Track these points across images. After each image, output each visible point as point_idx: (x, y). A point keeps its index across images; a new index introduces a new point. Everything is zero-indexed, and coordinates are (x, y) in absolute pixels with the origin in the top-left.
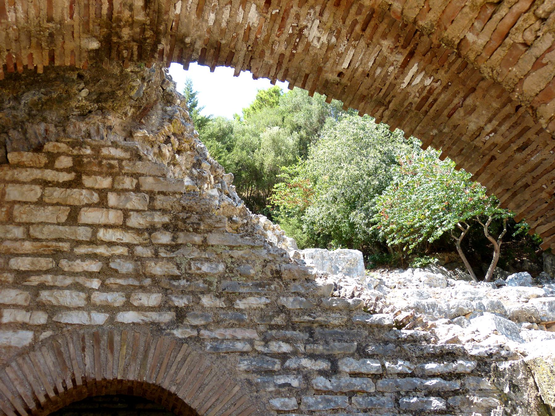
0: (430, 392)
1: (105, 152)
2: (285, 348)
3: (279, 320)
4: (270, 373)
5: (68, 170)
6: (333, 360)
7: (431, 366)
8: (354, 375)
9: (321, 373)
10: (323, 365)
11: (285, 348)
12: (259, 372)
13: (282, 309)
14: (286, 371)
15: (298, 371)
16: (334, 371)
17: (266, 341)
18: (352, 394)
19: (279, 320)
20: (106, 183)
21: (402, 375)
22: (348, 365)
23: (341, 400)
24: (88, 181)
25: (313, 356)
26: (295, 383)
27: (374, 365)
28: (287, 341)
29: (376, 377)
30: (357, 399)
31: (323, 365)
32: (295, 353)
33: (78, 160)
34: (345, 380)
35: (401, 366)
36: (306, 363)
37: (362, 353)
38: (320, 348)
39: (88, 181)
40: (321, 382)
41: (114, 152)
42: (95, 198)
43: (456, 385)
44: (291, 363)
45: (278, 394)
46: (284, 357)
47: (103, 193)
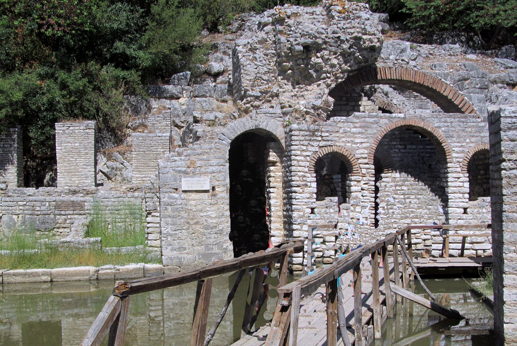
0: (427, 153)
1: (353, 95)
2: (395, 143)
3: (394, 137)
4: (392, 149)
5: (345, 101)
6: (405, 145)
7: (427, 147)
8: (410, 149)
9: (403, 148)
10: (403, 147)
11: (395, 143)
12: (389, 148)
13: (394, 134)
14: (395, 148)
15: (398, 148)
16: (405, 148)
17: (391, 141)
18: (409, 153)
19: (394, 137)
20: (354, 104)
21: (420, 149)
22: (409, 147)
23: (407, 154)
24: (350, 104)
25: (400, 145)
26: (397, 151)
27: (414, 147)
28: (396, 141)
29: (414, 149)
30: (410, 154)
31: (403, 147)
32: (397, 144)
33: (347, 98)
34: (408, 150)
35: (421, 147)
36: (399, 146)
37: (412, 144)
38: (402, 143)
39: (350, 104)
40: (403, 151)
41: (355, 95)
42: (352, 108)
43: (433, 151)
44: (396, 147)
45: (393, 153)
46: (395, 145)
47: (354, 106)
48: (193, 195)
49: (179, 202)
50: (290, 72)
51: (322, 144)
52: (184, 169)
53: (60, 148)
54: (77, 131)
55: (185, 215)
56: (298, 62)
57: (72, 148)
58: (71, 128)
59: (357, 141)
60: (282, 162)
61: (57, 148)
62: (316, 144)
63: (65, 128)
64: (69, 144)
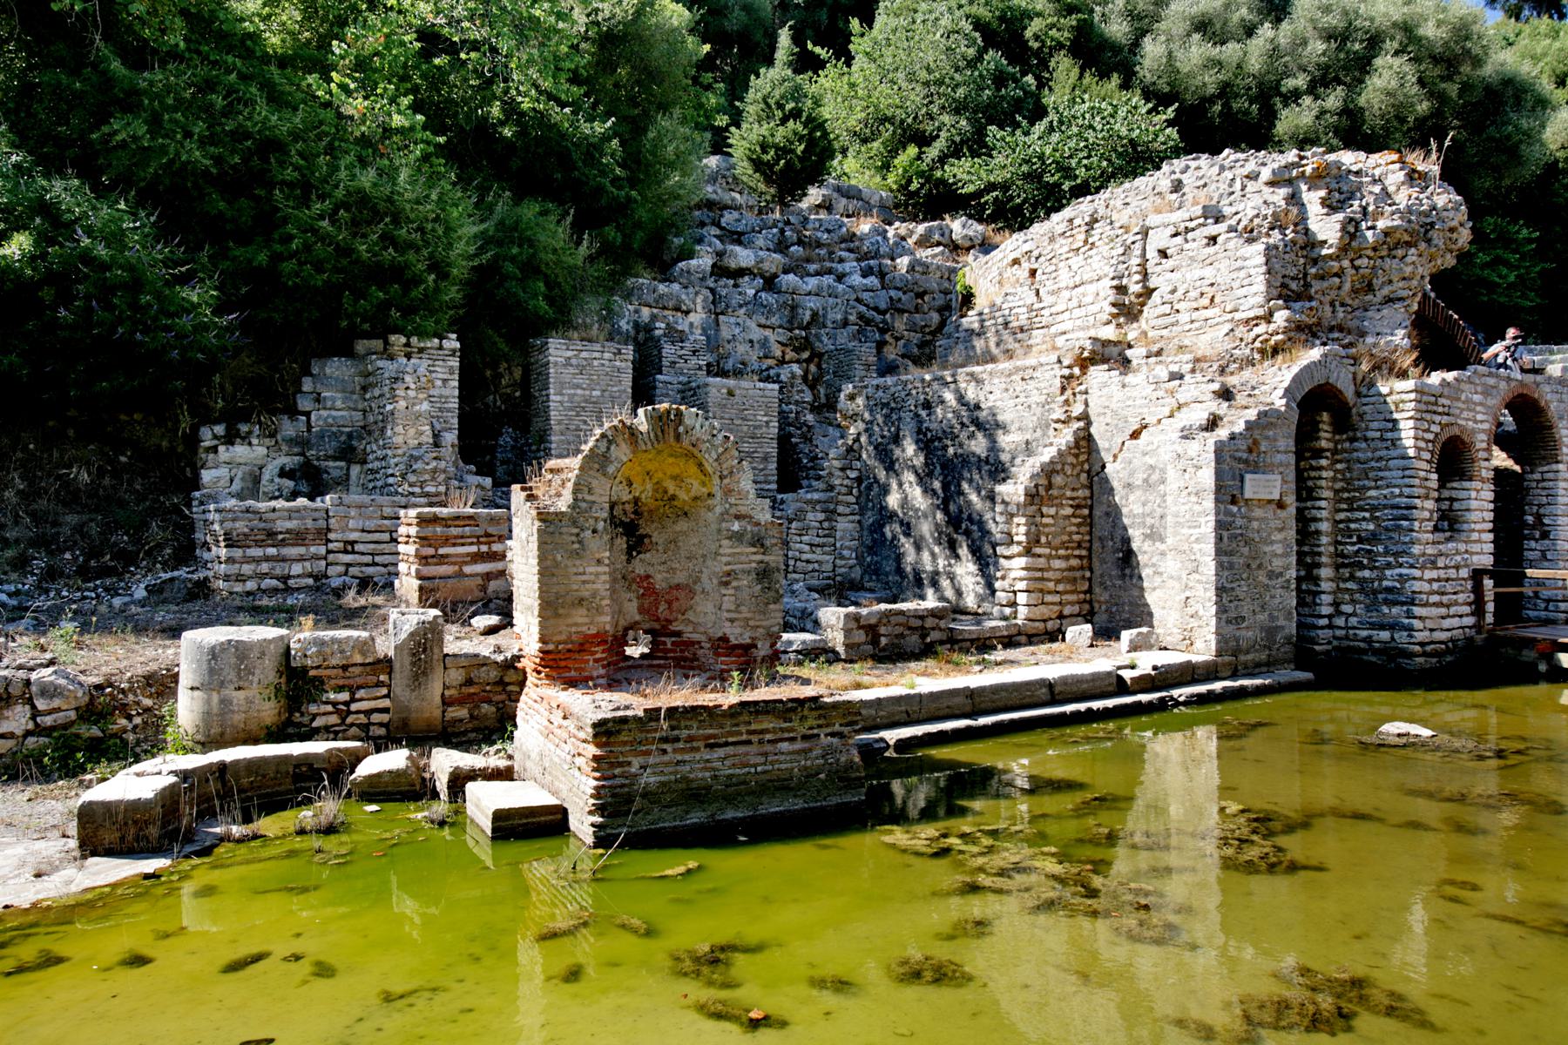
48: (1258, 513)
49: (1239, 522)
50: (1337, 280)
51: (1445, 419)
52: (1245, 456)
53: (558, 398)
54: (596, 363)
55: (1246, 550)
56: (1357, 263)
57: (586, 401)
58: (584, 355)
59: (1479, 417)
60: (1335, 452)
61: (552, 397)
62: (1437, 418)
63: (570, 354)
64: (579, 392)
